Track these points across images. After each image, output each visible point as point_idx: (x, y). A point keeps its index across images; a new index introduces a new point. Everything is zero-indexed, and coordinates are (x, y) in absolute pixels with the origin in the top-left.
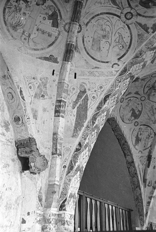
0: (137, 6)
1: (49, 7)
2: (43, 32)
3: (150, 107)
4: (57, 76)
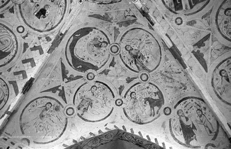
3: (161, 76)
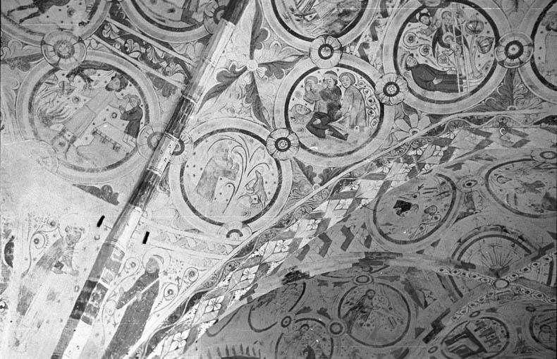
0: (301, 130)
1: (129, 98)
2: (104, 140)
4: (106, 229)
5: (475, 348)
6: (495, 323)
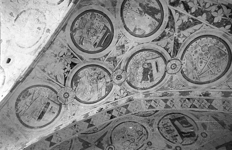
5: (176, 122)
6: (166, 136)
